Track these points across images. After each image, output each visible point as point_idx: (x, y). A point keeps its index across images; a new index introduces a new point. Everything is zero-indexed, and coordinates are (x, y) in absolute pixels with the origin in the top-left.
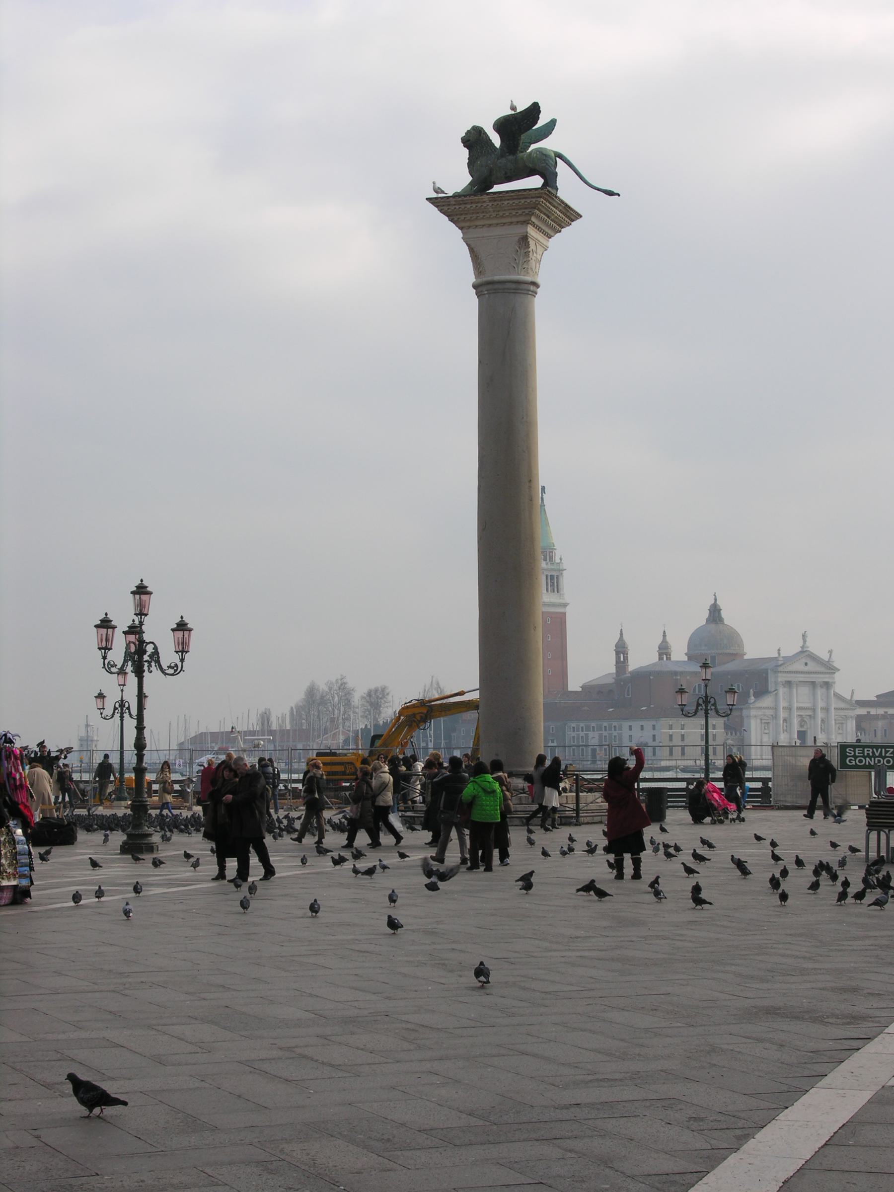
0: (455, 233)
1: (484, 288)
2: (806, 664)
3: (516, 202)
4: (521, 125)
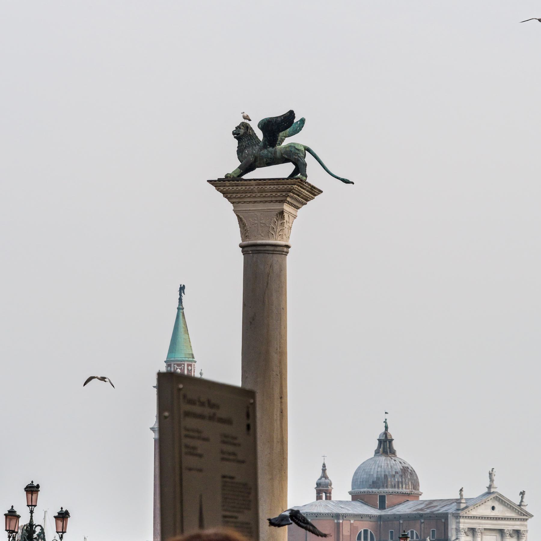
0: (226, 207)
1: (250, 249)
2: (493, 508)
3: (276, 187)
4: (280, 125)
